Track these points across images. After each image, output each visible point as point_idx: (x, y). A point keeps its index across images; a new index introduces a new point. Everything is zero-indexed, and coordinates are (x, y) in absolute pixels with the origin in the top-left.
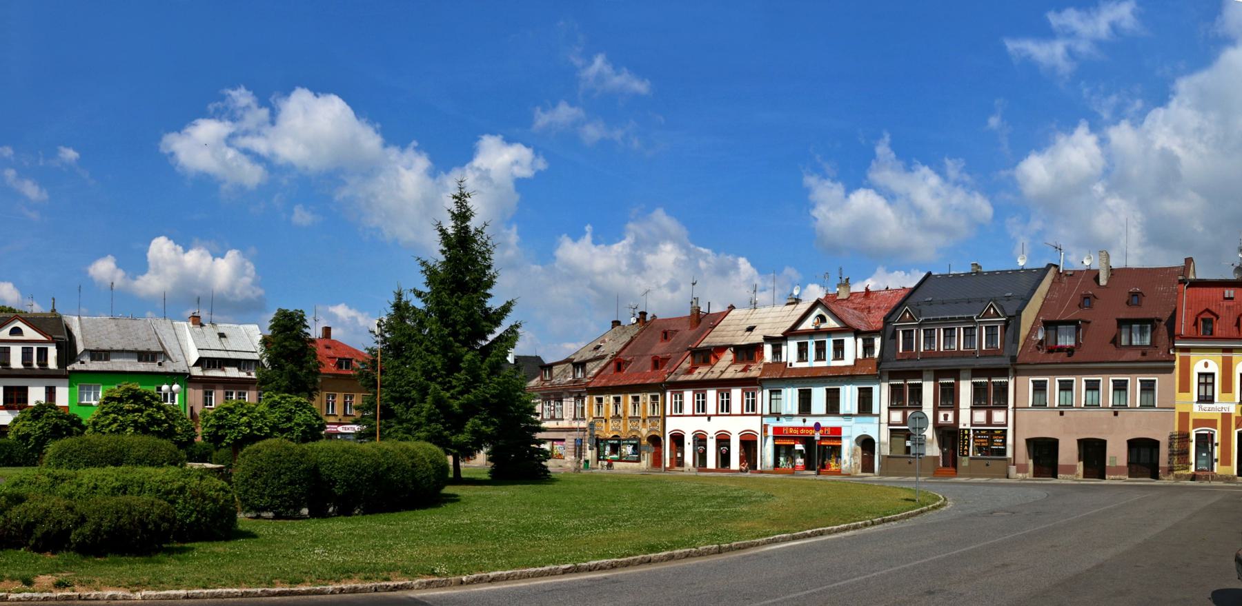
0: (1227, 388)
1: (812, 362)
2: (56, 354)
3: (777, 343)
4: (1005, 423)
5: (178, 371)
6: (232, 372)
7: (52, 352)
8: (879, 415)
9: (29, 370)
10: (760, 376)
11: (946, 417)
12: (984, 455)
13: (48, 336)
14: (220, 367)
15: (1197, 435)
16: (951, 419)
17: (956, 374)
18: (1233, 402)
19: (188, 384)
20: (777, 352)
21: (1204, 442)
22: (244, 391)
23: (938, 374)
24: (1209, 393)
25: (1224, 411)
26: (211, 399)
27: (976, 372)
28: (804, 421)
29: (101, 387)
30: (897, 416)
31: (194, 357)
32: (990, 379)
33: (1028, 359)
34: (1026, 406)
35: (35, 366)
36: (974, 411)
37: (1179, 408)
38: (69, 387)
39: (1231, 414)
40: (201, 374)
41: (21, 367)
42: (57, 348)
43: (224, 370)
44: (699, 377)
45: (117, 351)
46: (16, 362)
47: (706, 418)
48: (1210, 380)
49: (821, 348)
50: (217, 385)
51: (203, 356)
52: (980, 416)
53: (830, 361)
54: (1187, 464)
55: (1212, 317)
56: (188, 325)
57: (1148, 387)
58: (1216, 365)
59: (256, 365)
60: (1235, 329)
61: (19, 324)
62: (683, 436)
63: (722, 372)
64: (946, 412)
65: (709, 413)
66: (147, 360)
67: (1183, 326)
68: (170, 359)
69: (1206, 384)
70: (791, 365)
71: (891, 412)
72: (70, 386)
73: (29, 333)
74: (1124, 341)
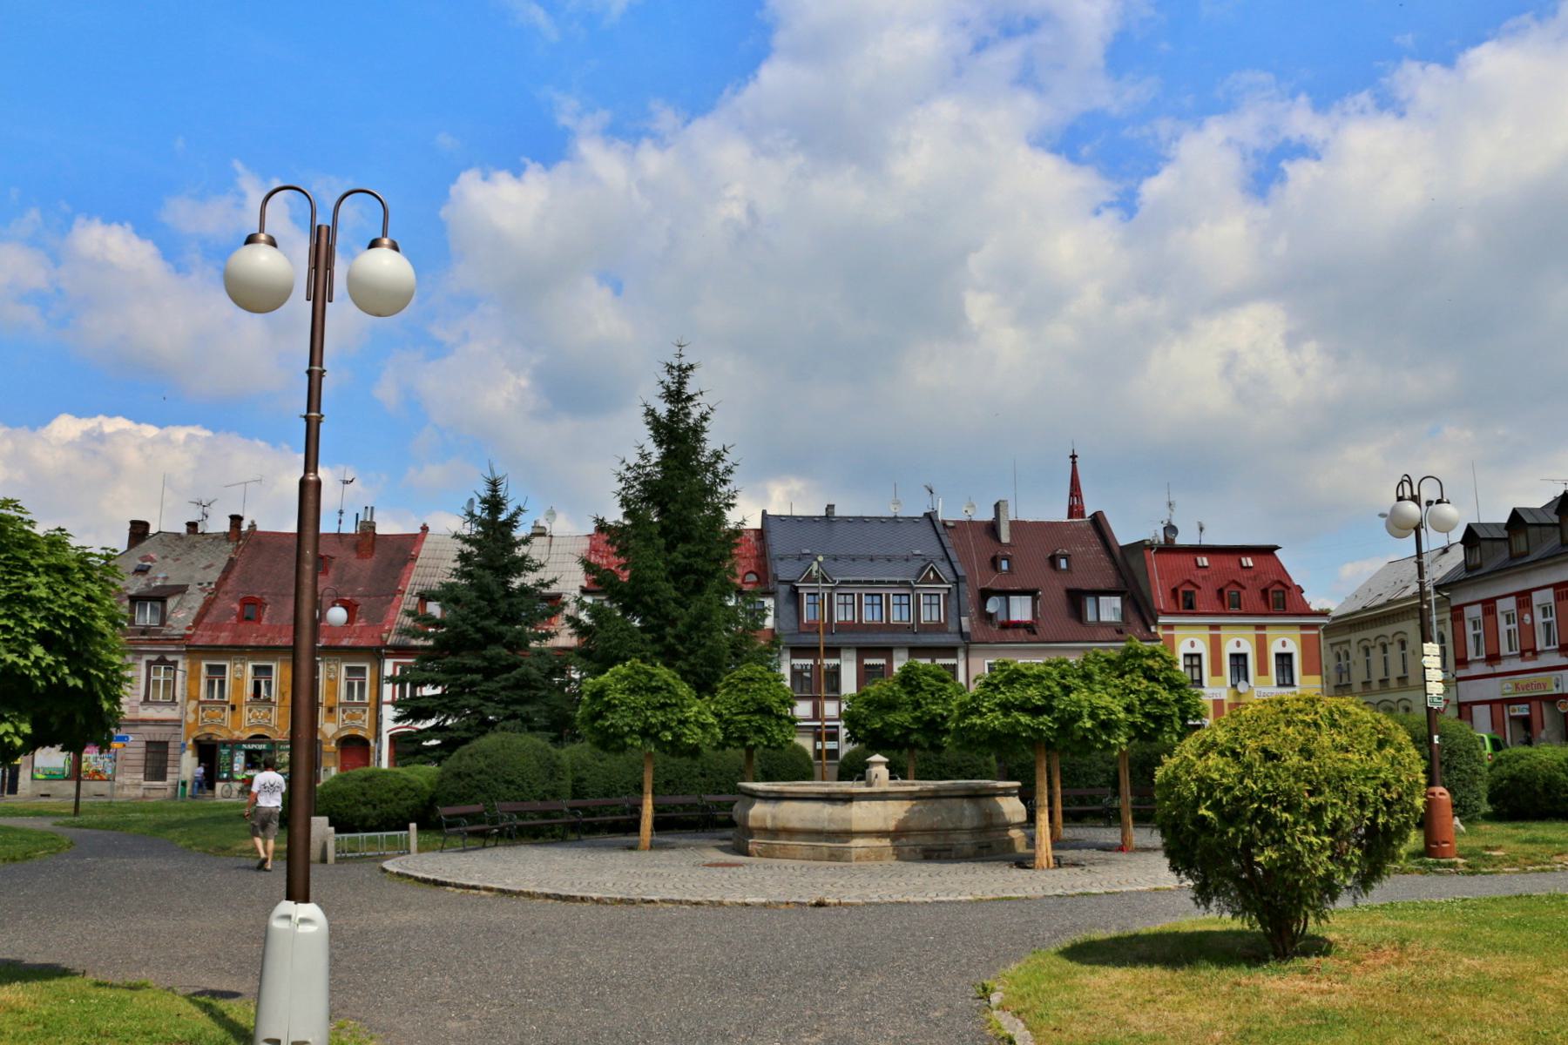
18: (1223, 686)
23: (863, 651)
24: (1196, 677)
32: (933, 661)
33: (980, 635)
39: (1222, 700)
48: (1196, 662)
55: (1192, 589)
58: (1203, 644)
60: (1217, 602)
67: (1160, 599)
69: (1192, 666)
74: (1091, 617)
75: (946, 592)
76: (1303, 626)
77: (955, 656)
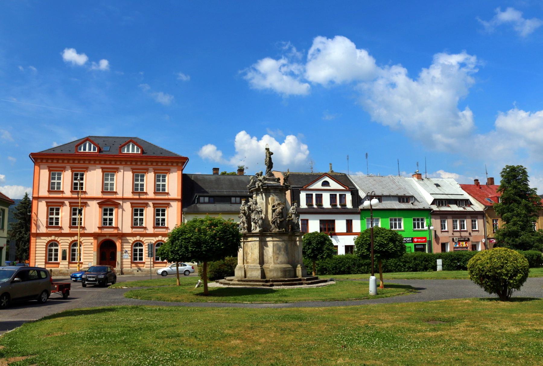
2: (351, 198)
5: (426, 208)
6: (454, 208)
7: (349, 197)
9: (335, 209)
13: (346, 187)
14: (446, 205)
19: (431, 216)
22: (456, 219)
26: (444, 225)
29: (380, 220)
31: (430, 199)
35: (339, 206)
38: (361, 220)
40: (437, 209)
41: (330, 207)
42: (351, 194)
43: (449, 207)
45: (386, 196)
46: (326, 203)
50: (448, 216)
51: (436, 198)
56: (414, 179)
59: (466, 202)
61: (327, 179)
66: (403, 202)
68: (418, 201)
72: (361, 219)
73: (334, 185)
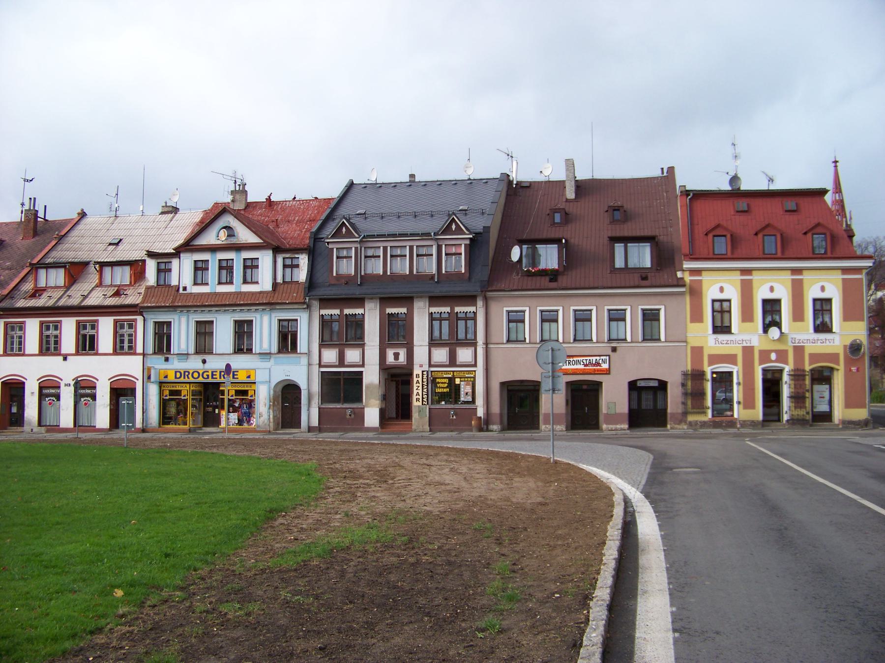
0: (747, 316)
1: (212, 286)
3: (163, 259)
4: (473, 363)
8: (309, 354)
10: (143, 302)
11: (396, 356)
12: (451, 403)
15: (713, 373)
16: (402, 359)
17: (407, 300)
20: (163, 271)
21: (723, 380)
25: (745, 344)
27: (434, 300)
28: (204, 362)
30: (330, 356)
34: (502, 342)
36: (432, 349)
37: (693, 342)
39: (753, 346)
44: (51, 303)
47: (61, 358)
49: (226, 268)
52: (441, 355)
53: (238, 286)
54: (702, 410)
57: (650, 317)
62: (24, 383)
63: (85, 297)
64: (397, 351)
65: (63, 351)
70: (185, 289)
71: (322, 350)
75: (468, 242)
76: (845, 270)
77: (475, 305)
